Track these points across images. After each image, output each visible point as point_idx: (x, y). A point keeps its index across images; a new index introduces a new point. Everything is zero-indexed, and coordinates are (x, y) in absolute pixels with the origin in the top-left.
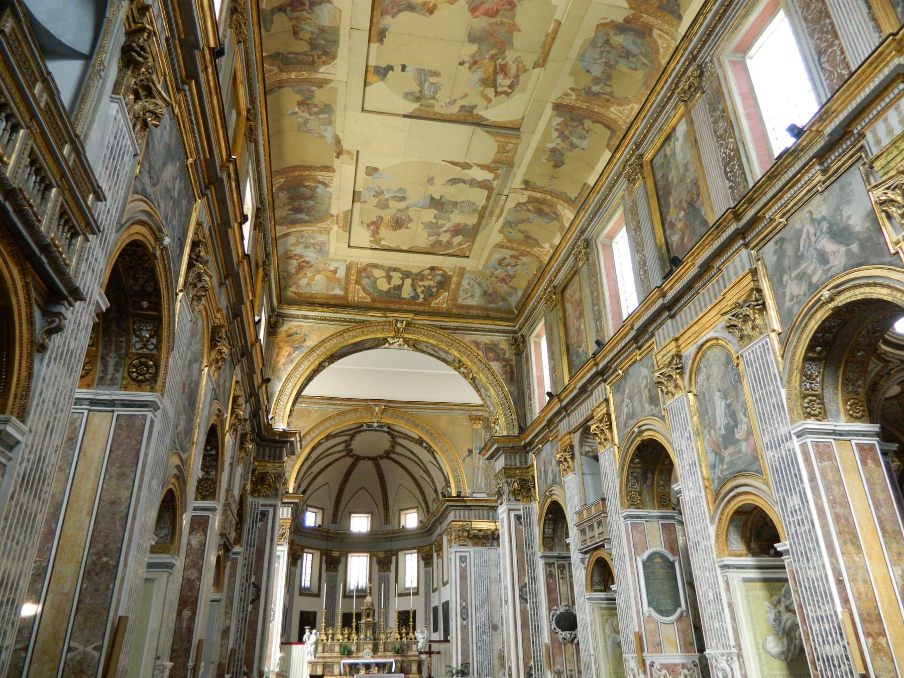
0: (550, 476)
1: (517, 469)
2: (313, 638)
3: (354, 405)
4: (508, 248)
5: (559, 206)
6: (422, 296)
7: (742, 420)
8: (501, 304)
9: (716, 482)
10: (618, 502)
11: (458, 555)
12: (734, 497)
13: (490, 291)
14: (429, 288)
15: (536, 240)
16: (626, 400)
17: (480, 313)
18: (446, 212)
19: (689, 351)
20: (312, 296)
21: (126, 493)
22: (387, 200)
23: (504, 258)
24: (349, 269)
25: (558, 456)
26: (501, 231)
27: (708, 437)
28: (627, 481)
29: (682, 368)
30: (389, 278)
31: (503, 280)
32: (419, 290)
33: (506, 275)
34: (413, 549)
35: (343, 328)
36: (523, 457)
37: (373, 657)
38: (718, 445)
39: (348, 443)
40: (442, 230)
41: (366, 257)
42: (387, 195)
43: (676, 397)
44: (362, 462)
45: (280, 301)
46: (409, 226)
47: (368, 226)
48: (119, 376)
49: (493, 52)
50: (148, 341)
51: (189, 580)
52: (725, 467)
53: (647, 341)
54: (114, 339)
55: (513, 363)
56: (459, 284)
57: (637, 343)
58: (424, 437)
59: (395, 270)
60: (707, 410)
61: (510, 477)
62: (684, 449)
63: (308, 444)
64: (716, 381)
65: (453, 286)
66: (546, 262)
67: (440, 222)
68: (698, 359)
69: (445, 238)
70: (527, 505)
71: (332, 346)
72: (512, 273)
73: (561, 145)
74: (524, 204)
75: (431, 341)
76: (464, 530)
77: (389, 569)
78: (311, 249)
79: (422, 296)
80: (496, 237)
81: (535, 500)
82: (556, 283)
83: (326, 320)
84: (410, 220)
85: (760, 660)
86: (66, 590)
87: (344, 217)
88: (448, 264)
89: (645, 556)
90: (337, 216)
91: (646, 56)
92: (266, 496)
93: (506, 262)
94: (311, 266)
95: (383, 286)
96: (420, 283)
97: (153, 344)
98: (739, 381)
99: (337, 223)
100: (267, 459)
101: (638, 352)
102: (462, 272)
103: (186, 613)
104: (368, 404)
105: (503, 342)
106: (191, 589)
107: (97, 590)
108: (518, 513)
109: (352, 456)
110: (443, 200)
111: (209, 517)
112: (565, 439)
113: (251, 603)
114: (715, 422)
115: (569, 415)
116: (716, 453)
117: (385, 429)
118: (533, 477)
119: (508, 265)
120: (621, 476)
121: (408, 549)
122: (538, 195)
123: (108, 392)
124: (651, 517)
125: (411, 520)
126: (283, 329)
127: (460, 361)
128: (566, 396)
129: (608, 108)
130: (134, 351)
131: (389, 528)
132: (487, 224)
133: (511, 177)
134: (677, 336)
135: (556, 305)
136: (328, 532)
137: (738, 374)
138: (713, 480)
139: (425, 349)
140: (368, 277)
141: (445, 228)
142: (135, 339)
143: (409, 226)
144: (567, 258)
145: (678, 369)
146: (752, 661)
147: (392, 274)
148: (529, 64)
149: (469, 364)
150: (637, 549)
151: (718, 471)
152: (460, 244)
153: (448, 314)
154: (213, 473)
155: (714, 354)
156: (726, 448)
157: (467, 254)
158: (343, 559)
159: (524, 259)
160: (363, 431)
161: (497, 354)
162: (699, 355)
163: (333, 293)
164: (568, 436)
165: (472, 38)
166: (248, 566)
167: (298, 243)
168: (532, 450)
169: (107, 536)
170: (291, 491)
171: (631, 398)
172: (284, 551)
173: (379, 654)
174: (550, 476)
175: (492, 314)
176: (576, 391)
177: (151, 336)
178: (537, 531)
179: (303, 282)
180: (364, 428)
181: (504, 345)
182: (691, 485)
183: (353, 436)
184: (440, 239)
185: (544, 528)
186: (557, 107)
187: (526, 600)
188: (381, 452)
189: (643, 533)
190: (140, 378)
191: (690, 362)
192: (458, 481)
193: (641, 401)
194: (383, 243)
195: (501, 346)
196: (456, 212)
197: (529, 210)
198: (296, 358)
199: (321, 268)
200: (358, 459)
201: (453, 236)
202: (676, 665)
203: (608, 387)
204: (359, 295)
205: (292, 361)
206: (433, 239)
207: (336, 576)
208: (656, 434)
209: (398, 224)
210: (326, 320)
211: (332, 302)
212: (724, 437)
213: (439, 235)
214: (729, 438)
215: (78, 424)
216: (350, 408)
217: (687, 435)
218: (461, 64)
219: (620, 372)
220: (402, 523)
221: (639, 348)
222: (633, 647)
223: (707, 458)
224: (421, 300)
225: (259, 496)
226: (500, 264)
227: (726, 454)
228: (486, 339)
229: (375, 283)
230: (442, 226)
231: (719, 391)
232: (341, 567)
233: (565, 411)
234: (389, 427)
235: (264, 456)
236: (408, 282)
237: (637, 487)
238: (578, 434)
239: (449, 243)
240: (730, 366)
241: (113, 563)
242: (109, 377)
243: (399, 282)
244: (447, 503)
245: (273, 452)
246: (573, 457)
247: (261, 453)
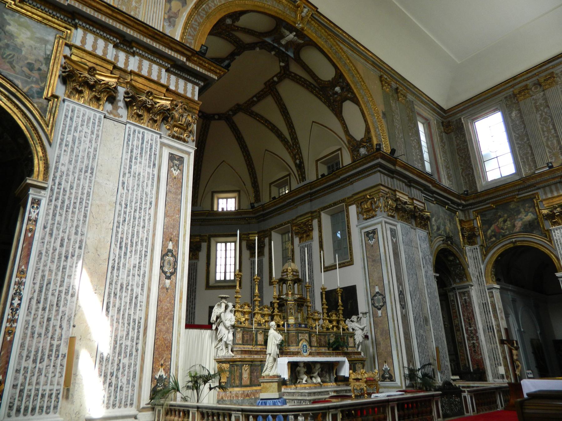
2: (229, 318)
37: (311, 354)
172: (189, 153)
244: (380, 160)
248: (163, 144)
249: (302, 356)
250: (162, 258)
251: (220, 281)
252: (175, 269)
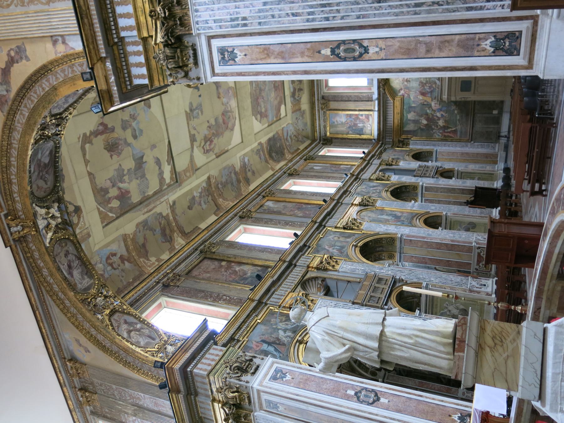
5: (175, 234)
15: (147, 252)
18: (135, 174)
22: (130, 126)
42: (134, 124)
46: (115, 157)
47: (102, 124)
49: (215, 132)
73: (197, 199)
74: (163, 217)
91: (237, 189)
110: (144, 165)
119: (111, 265)
122: (171, 218)
129: (219, 198)
132: (140, 210)
133: (174, 191)
141: (121, 185)
143: (115, 157)
148: (215, 152)
165: (216, 120)
186: (209, 178)
196: (138, 181)
197: (160, 224)
201: (117, 198)
218: (208, 122)
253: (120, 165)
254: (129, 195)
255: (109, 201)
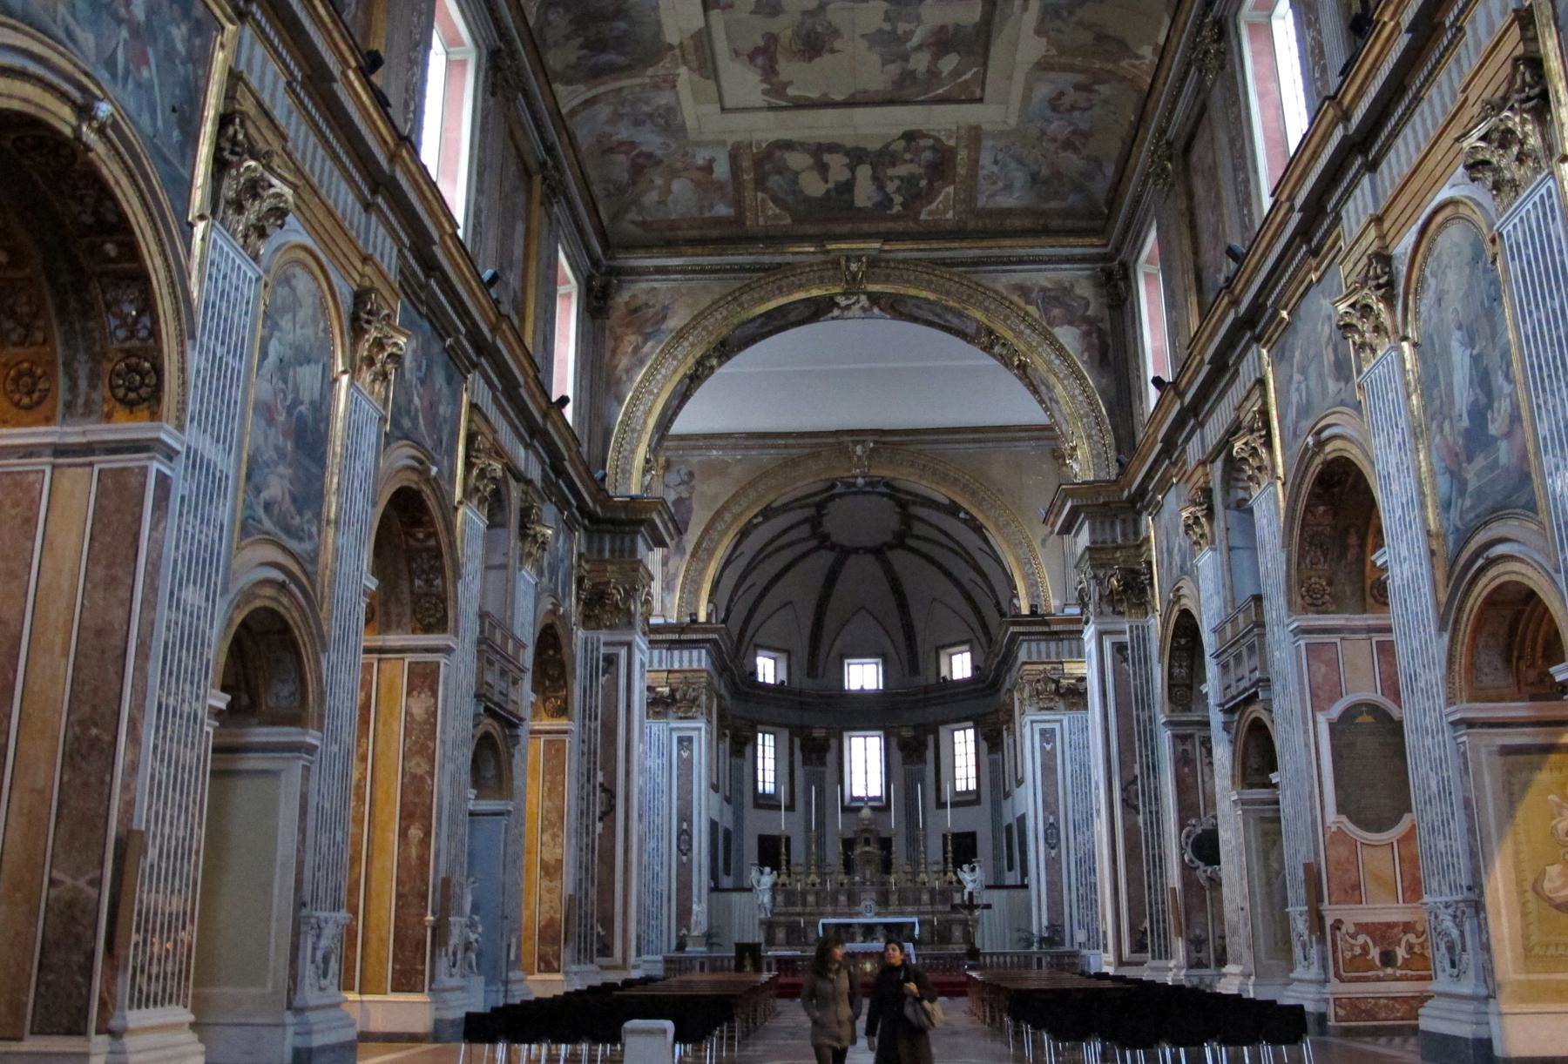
0: (1177, 559)
1: (1117, 548)
3: (812, 446)
4: (1064, 68)
6: (898, 199)
7: (1501, 389)
8: (1072, 199)
9: (1451, 538)
10: (1282, 601)
11: (1037, 727)
12: (1482, 570)
13: (1045, 172)
14: (910, 180)
15: (1121, 43)
16: (1297, 377)
17: (1028, 223)
19: (1403, 246)
20: (673, 225)
21: (120, 613)
23: (1062, 94)
24: (734, 157)
25: (1185, 514)
26: (1040, 31)
27: (1438, 439)
28: (1302, 556)
29: (1391, 284)
30: (823, 169)
31: (1068, 145)
32: (891, 187)
33: (1074, 132)
34: (966, 719)
35: (739, 284)
36: (1130, 523)
38: (1457, 455)
39: (815, 522)
40: (909, 45)
41: (766, 128)
43: (1380, 353)
44: (853, 559)
45: (606, 245)
46: (837, 45)
47: (752, 58)
48: (96, 396)
50: (136, 320)
51: (414, 776)
52: (1468, 503)
53: (1328, 233)
54: (77, 326)
55: (1106, 326)
56: (974, 163)
57: (1309, 242)
58: (959, 500)
59: (833, 148)
60: (1437, 375)
61: (1102, 566)
62: (1393, 471)
63: (728, 528)
64: (1454, 307)
65: (962, 171)
66: (1146, 87)
67: (902, 27)
68: (1419, 258)
69: (920, 62)
70: (1139, 622)
71: (719, 326)
72: (1084, 126)
75: (924, 294)
76: (1048, 680)
77: (922, 759)
78: (649, 126)
79: (898, 199)
80: (1032, 48)
81: (1154, 610)
82: (1171, 133)
83: (702, 270)
84: (836, 33)
85: (1524, 915)
86: (40, 784)
87: (696, 49)
88: (942, 120)
89: (1336, 710)
90: (681, 45)
92: (612, 627)
93: (1067, 101)
94: (659, 163)
95: (814, 186)
96: (890, 172)
97: (145, 327)
98: (1497, 299)
99: (685, 62)
100: (607, 555)
101: (1314, 263)
102: (975, 135)
103: (415, 832)
104: (837, 442)
105: (1080, 282)
106: (418, 793)
107: (85, 784)
108: (1118, 638)
109: (833, 547)
111: (438, 664)
112: (1195, 478)
113: (601, 819)
114: (1452, 402)
115: (1201, 425)
116: (1452, 474)
117: (882, 489)
118: (1149, 564)
119: (1073, 108)
120: (1287, 544)
121: (958, 721)
123: (78, 429)
124: (1354, 630)
125: (961, 666)
126: (622, 299)
127: (990, 332)
128: (1190, 383)
130: (116, 344)
131: (920, 681)
134: (1379, 212)
135: (1172, 185)
136: (800, 693)
137: (1495, 282)
138: (1445, 537)
139: (917, 312)
140: (780, 172)
141: (915, 41)
142: (114, 322)
143: (837, 45)
144: (1186, 73)
145: (1378, 287)
146: (1504, 919)
147: (827, 158)
149: (1009, 335)
150: (1320, 696)
151: (1454, 513)
152: (956, 73)
153: (958, 233)
154: (438, 582)
155: (1452, 240)
156: (1470, 460)
157: (978, 94)
158: (834, 743)
159: (1104, 90)
160: (840, 495)
161: (1068, 308)
162: (1422, 249)
163: (713, 214)
164: (1200, 471)
166: (588, 754)
167: (617, 117)
168: (1147, 508)
169: (95, 691)
170: (702, 617)
171: (1304, 371)
172: (699, 729)
173: (891, 908)
174: (1177, 559)
175: (1055, 223)
176: (1206, 369)
177: (140, 314)
178: (1159, 674)
179: (651, 198)
180: (840, 489)
181: (1085, 290)
182: (1404, 553)
183: (820, 506)
184: (911, 66)
185: (1170, 667)
187: (1136, 808)
188: (888, 538)
189: (1334, 664)
190: (132, 395)
191: (1404, 269)
192: (1033, 585)
193: (1321, 375)
194: (791, 92)
195: (1078, 291)
198: (648, 355)
199: (679, 165)
200: (844, 553)
201: (937, 57)
202: (1390, 926)
203: (1264, 351)
204: (767, 213)
205: (642, 362)
206: (894, 69)
207: (824, 773)
208: (1349, 446)
209: (813, 44)
210: (702, 270)
211: (715, 233)
212: (1467, 433)
213: (905, 58)
214: (1477, 438)
215: (36, 493)
216: (807, 451)
217: (1398, 438)
219: (1284, 314)
220: (944, 672)
221: (1315, 253)
222: (1302, 892)
223: (1434, 487)
224: (897, 208)
225: (598, 627)
226: (1054, 109)
227: (1470, 473)
228: (1043, 278)
229: (795, 181)
230: (908, 35)
231: (1460, 327)
232: (831, 757)
233: (1193, 414)
234: (887, 485)
235: (601, 551)
236: (864, 172)
237: (1323, 567)
238: (1219, 463)
239: (933, 74)
240: (1480, 265)
241: (107, 738)
242: (81, 400)
243: (845, 175)
244: (1012, 629)
245: (618, 543)
246: (1210, 514)
247: (595, 546)
248: (672, 730)
249: (865, 917)
250: (678, 839)
251: (962, 793)
252: (691, 845)
253: (863, 36)
254: (951, 29)
255: (933, 74)
